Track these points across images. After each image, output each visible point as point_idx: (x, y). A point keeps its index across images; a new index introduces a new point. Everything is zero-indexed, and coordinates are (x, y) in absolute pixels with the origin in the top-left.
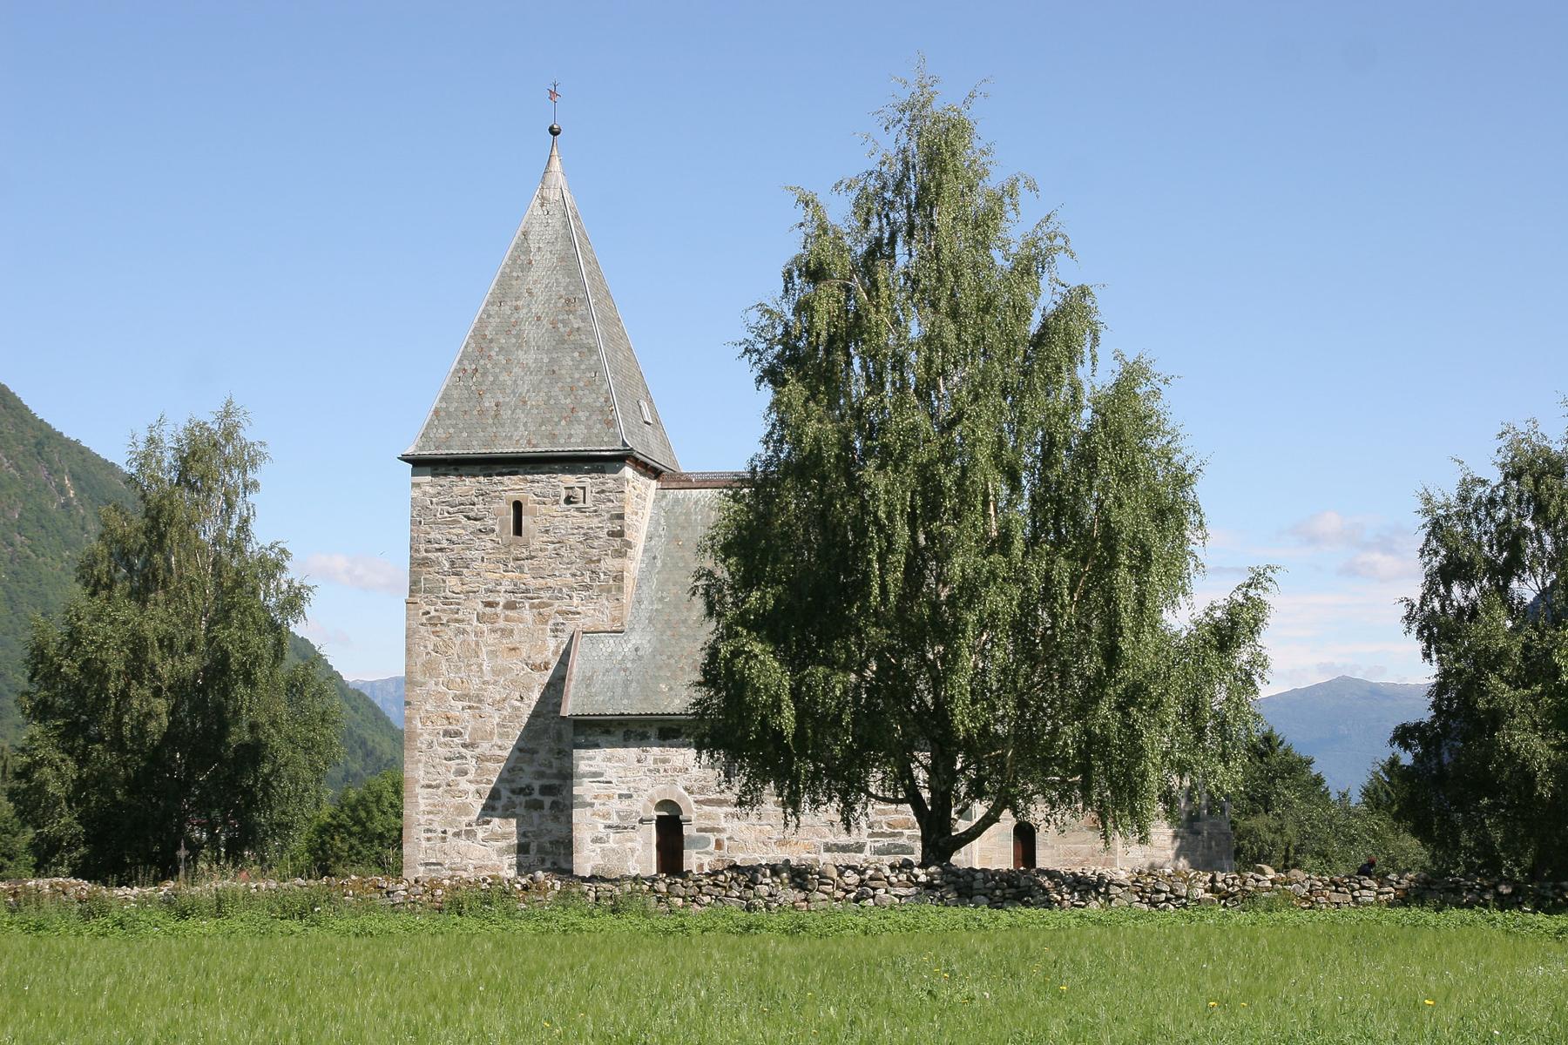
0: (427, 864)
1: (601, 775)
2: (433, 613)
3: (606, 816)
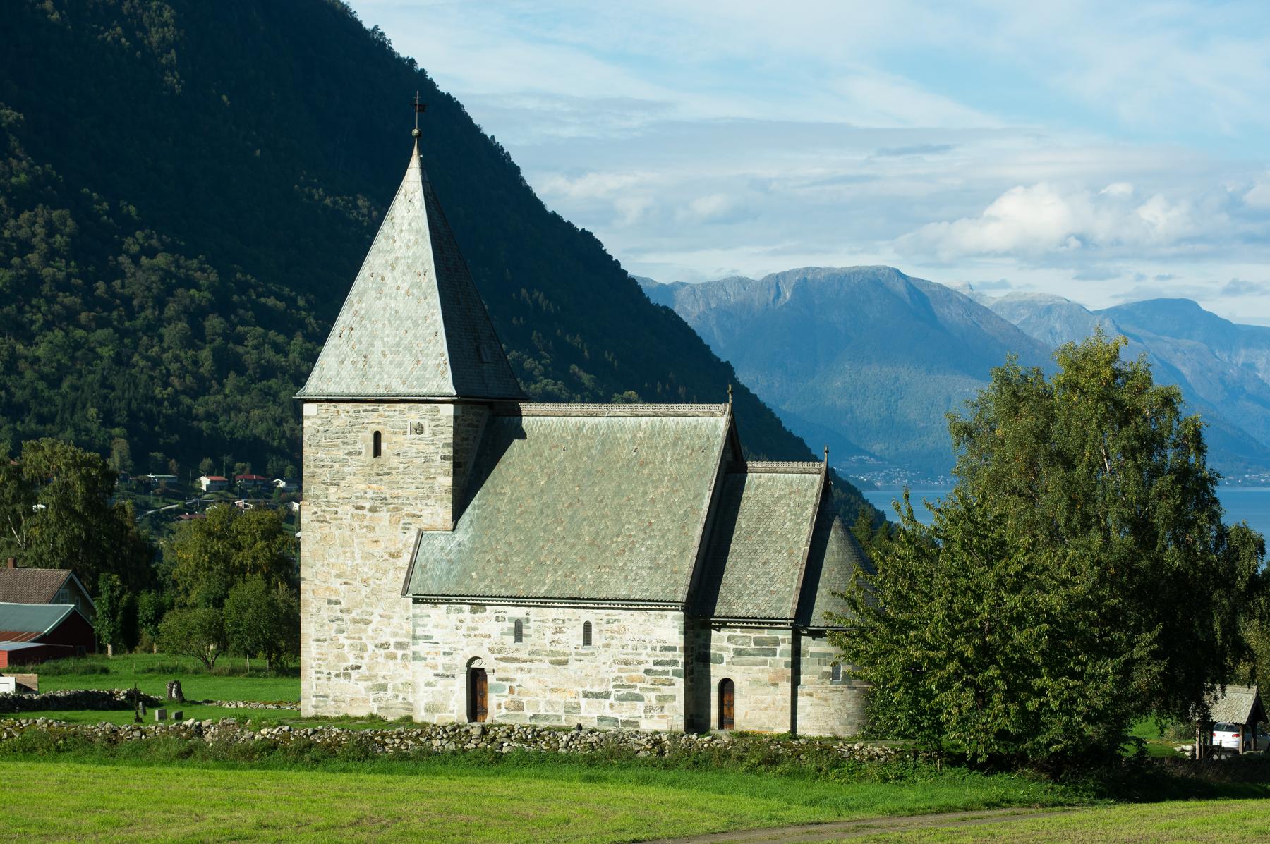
0: (317, 696)
1: (432, 637)
2: (319, 513)
3: (434, 667)
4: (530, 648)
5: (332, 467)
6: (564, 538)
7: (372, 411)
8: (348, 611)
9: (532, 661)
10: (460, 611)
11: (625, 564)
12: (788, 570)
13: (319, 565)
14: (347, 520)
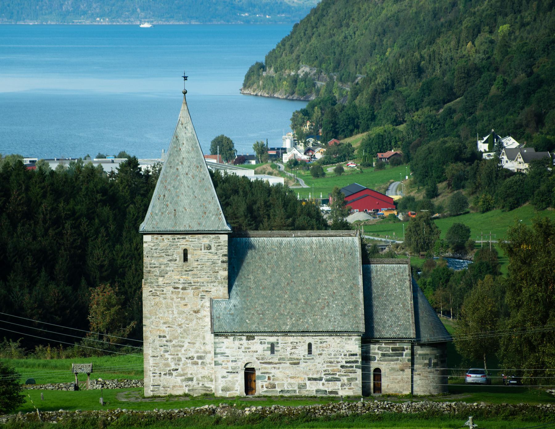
0: (153, 386)
1: (225, 353)
3: (227, 368)
4: (279, 357)
5: (160, 267)
6: (290, 301)
7: (182, 238)
8: (171, 341)
9: (280, 363)
10: (241, 339)
11: (327, 314)
12: (405, 314)
13: (153, 318)
14: (169, 295)
